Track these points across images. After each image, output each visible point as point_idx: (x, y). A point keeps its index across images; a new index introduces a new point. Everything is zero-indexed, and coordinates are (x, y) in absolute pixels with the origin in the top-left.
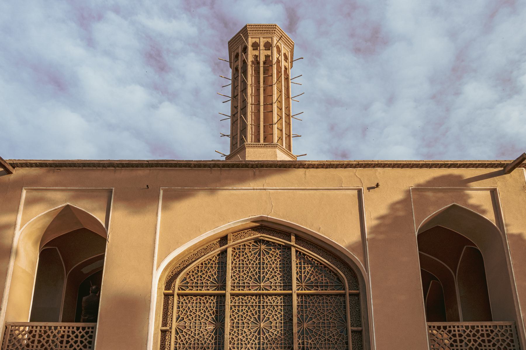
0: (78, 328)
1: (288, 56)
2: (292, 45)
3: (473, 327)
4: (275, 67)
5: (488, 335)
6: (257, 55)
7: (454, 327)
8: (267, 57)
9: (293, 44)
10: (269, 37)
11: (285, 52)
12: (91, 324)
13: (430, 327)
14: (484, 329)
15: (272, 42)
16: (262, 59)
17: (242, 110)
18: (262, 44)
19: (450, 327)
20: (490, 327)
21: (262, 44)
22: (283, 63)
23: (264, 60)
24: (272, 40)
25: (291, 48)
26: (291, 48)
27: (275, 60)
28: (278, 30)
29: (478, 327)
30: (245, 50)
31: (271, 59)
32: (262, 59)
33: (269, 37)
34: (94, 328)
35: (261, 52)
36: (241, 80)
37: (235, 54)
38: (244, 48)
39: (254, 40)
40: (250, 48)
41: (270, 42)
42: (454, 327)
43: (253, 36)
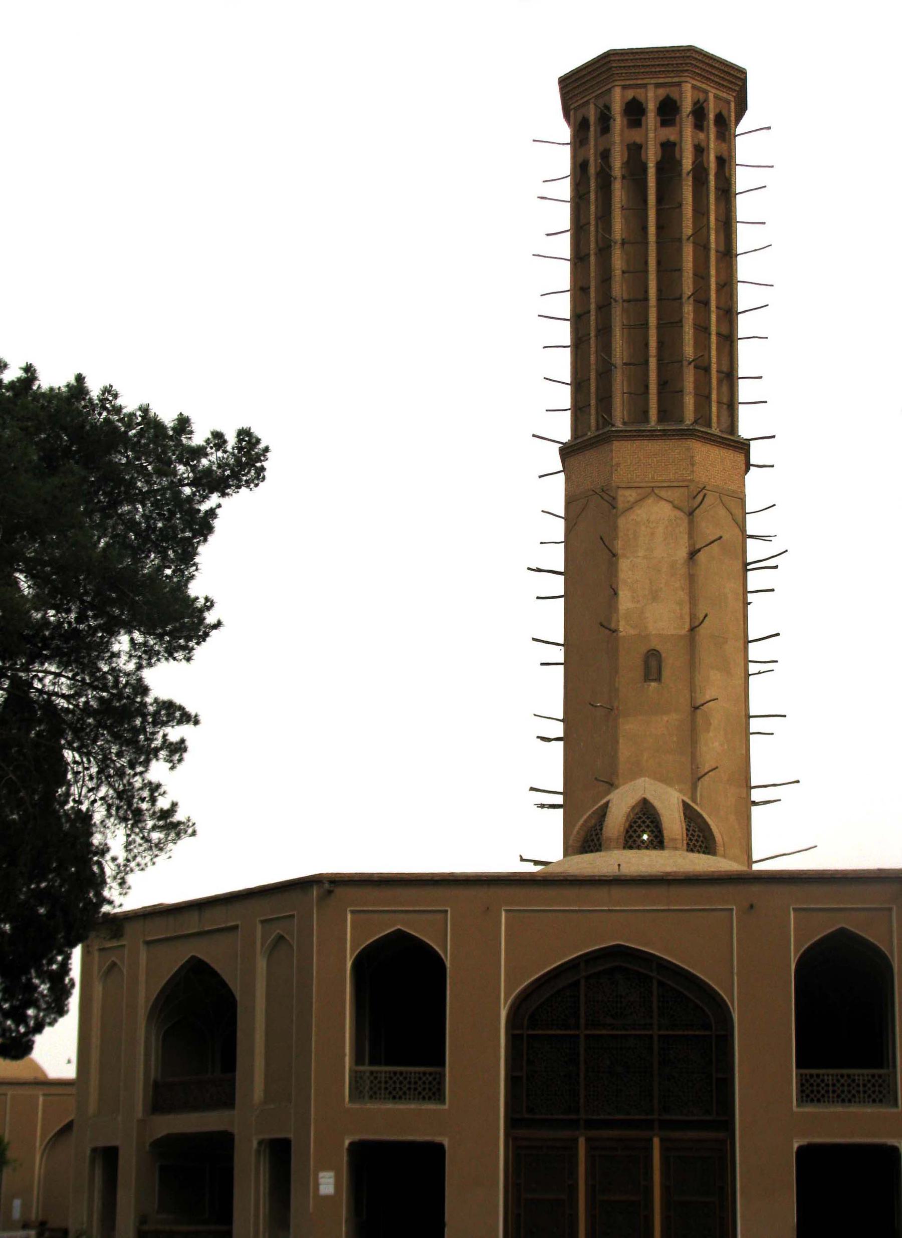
0: (424, 1074)
1: (729, 116)
2: (742, 79)
3: (849, 1076)
4: (690, 183)
5: (864, 1085)
6: (638, 140)
7: (828, 1075)
8: (669, 149)
9: (742, 77)
10: (673, 84)
11: (718, 111)
12: (438, 1069)
13: (801, 1075)
14: (861, 1078)
15: (681, 98)
16: (652, 156)
17: (600, 375)
18: (651, 107)
19: (823, 1075)
20: (868, 1075)
21: (651, 107)
22: (713, 149)
23: (659, 159)
24: (681, 93)
25: (737, 88)
26: (737, 88)
27: (687, 163)
28: (696, 59)
29: (854, 1075)
30: (605, 119)
31: (678, 156)
32: (652, 156)
33: (673, 84)
34: (442, 1076)
35: (651, 135)
36: (596, 214)
37: (580, 118)
38: (602, 154)
39: (630, 94)
40: (618, 121)
41: (675, 96)
42: (828, 1075)
43: (628, 83)
